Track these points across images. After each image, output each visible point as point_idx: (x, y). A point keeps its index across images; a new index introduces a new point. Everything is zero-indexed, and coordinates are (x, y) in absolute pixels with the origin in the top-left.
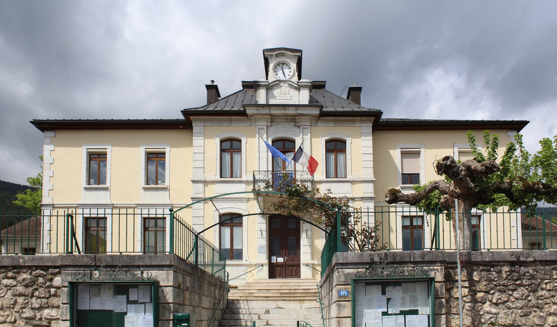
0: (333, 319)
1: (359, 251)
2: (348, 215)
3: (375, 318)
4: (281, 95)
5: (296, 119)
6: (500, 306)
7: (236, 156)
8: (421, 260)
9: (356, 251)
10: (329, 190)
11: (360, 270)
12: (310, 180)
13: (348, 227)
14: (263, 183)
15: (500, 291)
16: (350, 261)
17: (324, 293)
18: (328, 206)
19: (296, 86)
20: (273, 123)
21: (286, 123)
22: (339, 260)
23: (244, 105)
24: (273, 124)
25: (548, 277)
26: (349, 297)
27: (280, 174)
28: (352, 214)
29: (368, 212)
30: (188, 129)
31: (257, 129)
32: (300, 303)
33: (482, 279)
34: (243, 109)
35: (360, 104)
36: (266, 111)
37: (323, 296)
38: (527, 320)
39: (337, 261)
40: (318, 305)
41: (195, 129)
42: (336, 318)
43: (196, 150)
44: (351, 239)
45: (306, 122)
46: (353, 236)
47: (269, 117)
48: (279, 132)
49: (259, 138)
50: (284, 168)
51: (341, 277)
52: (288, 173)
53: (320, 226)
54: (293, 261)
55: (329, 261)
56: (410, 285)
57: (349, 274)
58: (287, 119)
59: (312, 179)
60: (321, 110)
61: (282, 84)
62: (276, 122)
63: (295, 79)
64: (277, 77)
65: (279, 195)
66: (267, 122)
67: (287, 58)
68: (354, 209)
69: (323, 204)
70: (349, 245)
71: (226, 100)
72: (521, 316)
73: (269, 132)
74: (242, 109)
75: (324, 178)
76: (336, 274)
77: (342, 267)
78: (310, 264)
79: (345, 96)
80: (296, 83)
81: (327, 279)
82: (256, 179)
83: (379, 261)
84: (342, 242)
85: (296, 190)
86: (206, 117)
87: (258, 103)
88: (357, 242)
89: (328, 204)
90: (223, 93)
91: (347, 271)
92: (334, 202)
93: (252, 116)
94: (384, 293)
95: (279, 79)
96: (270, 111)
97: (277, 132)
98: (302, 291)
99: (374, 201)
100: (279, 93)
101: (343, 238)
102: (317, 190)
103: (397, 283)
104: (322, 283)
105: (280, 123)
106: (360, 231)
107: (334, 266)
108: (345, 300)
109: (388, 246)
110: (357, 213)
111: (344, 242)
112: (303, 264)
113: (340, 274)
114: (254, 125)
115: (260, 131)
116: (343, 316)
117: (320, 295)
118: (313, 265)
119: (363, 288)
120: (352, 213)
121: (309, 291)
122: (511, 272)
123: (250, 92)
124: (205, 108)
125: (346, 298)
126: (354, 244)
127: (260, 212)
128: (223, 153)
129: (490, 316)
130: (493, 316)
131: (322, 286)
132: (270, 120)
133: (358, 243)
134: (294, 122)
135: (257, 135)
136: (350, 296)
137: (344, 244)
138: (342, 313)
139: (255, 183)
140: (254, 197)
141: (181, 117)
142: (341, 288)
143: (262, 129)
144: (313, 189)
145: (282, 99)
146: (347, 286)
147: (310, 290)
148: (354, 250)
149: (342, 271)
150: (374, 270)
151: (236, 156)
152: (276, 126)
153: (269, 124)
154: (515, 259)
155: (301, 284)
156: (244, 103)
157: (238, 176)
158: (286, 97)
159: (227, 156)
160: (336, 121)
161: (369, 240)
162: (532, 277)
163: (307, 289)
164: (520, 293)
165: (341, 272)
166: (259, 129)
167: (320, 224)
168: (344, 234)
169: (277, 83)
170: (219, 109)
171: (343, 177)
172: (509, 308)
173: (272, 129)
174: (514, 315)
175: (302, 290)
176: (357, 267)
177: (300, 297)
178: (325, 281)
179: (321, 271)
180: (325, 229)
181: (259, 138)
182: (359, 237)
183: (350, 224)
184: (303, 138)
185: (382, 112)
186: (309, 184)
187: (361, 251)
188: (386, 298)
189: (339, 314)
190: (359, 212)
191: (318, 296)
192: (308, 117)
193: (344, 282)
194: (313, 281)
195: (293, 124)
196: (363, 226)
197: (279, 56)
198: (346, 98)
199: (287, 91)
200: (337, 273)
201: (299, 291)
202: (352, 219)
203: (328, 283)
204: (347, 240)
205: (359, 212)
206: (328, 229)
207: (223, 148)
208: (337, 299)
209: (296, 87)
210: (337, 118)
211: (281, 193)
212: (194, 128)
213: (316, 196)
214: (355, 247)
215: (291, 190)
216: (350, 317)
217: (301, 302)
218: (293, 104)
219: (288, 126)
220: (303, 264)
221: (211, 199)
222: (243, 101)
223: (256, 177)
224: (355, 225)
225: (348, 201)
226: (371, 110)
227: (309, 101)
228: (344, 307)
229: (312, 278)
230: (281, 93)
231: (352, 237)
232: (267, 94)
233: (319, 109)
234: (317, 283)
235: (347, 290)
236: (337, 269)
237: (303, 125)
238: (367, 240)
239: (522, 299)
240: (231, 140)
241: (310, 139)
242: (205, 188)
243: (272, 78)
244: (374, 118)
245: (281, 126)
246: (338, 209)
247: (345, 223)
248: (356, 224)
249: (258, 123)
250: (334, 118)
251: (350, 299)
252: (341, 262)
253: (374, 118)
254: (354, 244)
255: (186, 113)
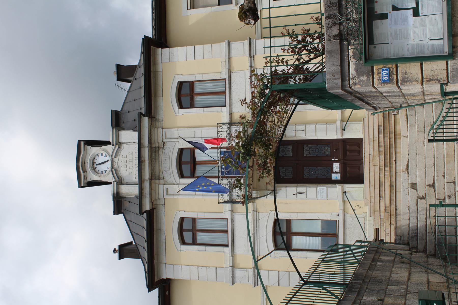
0: (425, 89)
1: (324, 56)
2: (274, 74)
3: (424, 26)
4: (128, 166)
5: (155, 148)
7: (200, 224)
9: (324, 60)
10: (242, 103)
11: (351, 54)
12: (229, 128)
13: (291, 73)
14: (234, 191)
16: (338, 69)
17: (384, 104)
18: (263, 102)
19: (117, 147)
20: (160, 176)
22: (337, 84)
23: (140, 213)
26: (392, 67)
27: (222, 168)
28: (273, 69)
29: (271, 47)
30: (169, 284)
31: (167, 197)
32: (400, 138)
34: (145, 214)
35: (136, 66)
36: (147, 185)
37: (389, 105)
39: (339, 88)
40: (402, 112)
41: (170, 276)
42: (422, 85)
43: (194, 277)
44: (307, 69)
45: (159, 134)
46: (302, 67)
47: (153, 180)
48: (171, 169)
49: (179, 195)
50: (214, 162)
51: (361, 81)
52: (221, 157)
53: (289, 112)
54: (339, 149)
55: (337, 98)
57: (356, 70)
58: (155, 159)
59: (227, 125)
60: (144, 116)
61: (116, 166)
62: (159, 173)
63: (109, 148)
64: (108, 170)
65: (249, 170)
66: (159, 184)
67: (87, 159)
68: (267, 66)
69: (260, 110)
70: (316, 70)
71: (135, 235)
73: (171, 182)
74: (145, 215)
75: (225, 110)
76: (357, 88)
77: (347, 79)
78: (341, 125)
79: (127, 85)
80: (114, 147)
81: (363, 101)
82: (229, 199)
83: (338, 26)
84: (311, 80)
85: (243, 146)
86: (155, 261)
87: (138, 195)
88: (311, 59)
89: (260, 103)
90: (127, 238)
91: (352, 71)
92: (258, 95)
93: (153, 203)
95: (110, 169)
96: (147, 181)
97: (171, 171)
98: (382, 136)
99: (254, 40)
100: (126, 169)
101: (305, 79)
102: (243, 118)
104: (370, 108)
105: (160, 168)
106: (296, 57)
107: (346, 91)
108: (395, 73)
109: (316, 16)
110: (271, 62)
111: (312, 78)
112: (342, 135)
113: (357, 82)
114: (163, 200)
115: (170, 193)
116: (420, 75)
117: (387, 109)
118: (342, 121)
119: (377, 48)
120: (271, 68)
121: (381, 126)
123: (126, 205)
124: (145, 262)
125: (392, 72)
126: (314, 65)
127: (271, 195)
128: (198, 242)
131: (374, 107)
132: (157, 181)
133: (313, 59)
134: (159, 150)
135: (175, 197)
136: (390, 66)
137: (314, 78)
138: (415, 77)
139: (234, 200)
140: (252, 203)
141: (156, 292)
142: (378, 80)
143: (167, 191)
144: (241, 124)
145: (132, 165)
146: (375, 71)
147: (380, 124)
148: (323, 63)
149: (353, 79)
150: (350, 33)
151: (200, 224)
152: (164, 172)
153: (162, 181)
155: (371, 137)
156: (138, 213)
157: (225, 223)
158: (130, 161)
159: (201, 237)
160: (156, 96)
161: (307, 43)
163: (379, 129)
165: (354, 81)
166: (167, 194)
167: (287, 113)
168: (300, 79)
169: (114, 170)
170: (145, 245)
171: (224, 83)
173: (167, 178)
175: (380, 136)
176: (346, 58)
177: (390, 138)
178: (367, 103)
179: (351, 110)
180: (294, 106)
181: (179, 195)
182: (304, 57)
183: (286, 71)
184: (178, 138)
185: (145, 36)
186: (233, 129)
187: (324, 54)
188: (392, 12)
189: (417, 81)
190: (271, 59)
191: (389, 113)
192: (152, 132)
193: (368, 75)
194: (366, 120)
195: (161, 150)
196: (288, 52)
197: (85, 169)
198: (130, 84)
199: (123, 159)
200: (356, 87)
201: (382, 140)
202: (280, 69)
203: (370, 99)
204: (309, 74)
205: (271, 59)
206: (294, 101)
207: (191, 242)
208: (395, 85)
209: (119, 148)
210: (153, 95)
211: (247, 167)
212: (169, 277)
213: (250, 119)
214: (319, 63)
215: (243, 154)
216: (421, 64)
217: (398, 137)
218: (138, 152)
219: (163, 157)
220: (342, 135)
221: (256, 262)
222: (136, 214)
223: (226, 200)
224: (287, 65)
225: (256, 75)
226: (143, 51)
227: (135, 131)
228: (406, 73)
229: (362, 122)
230: (125, 166)
231: (305, 67)
232: (127, 184)
233: (143, 117)
234: (370, 115)
235: (380, 71)
236: (349, 87)
237: (162, 138)
238: (308, 46)
240: (181, 231)
241: (179, 129)
242: (241, 266)
243: (109, 178)
244: (152, 47)
245: (164, 166)
246: (266, 89)
247: (285, 77)
248: (287, 63)
249: (161, 197)
250: (152, 98)
251: (394, 66)
252: (339, 81)
253: (152, 47)
254: (314, 65)
255: (151, 287)
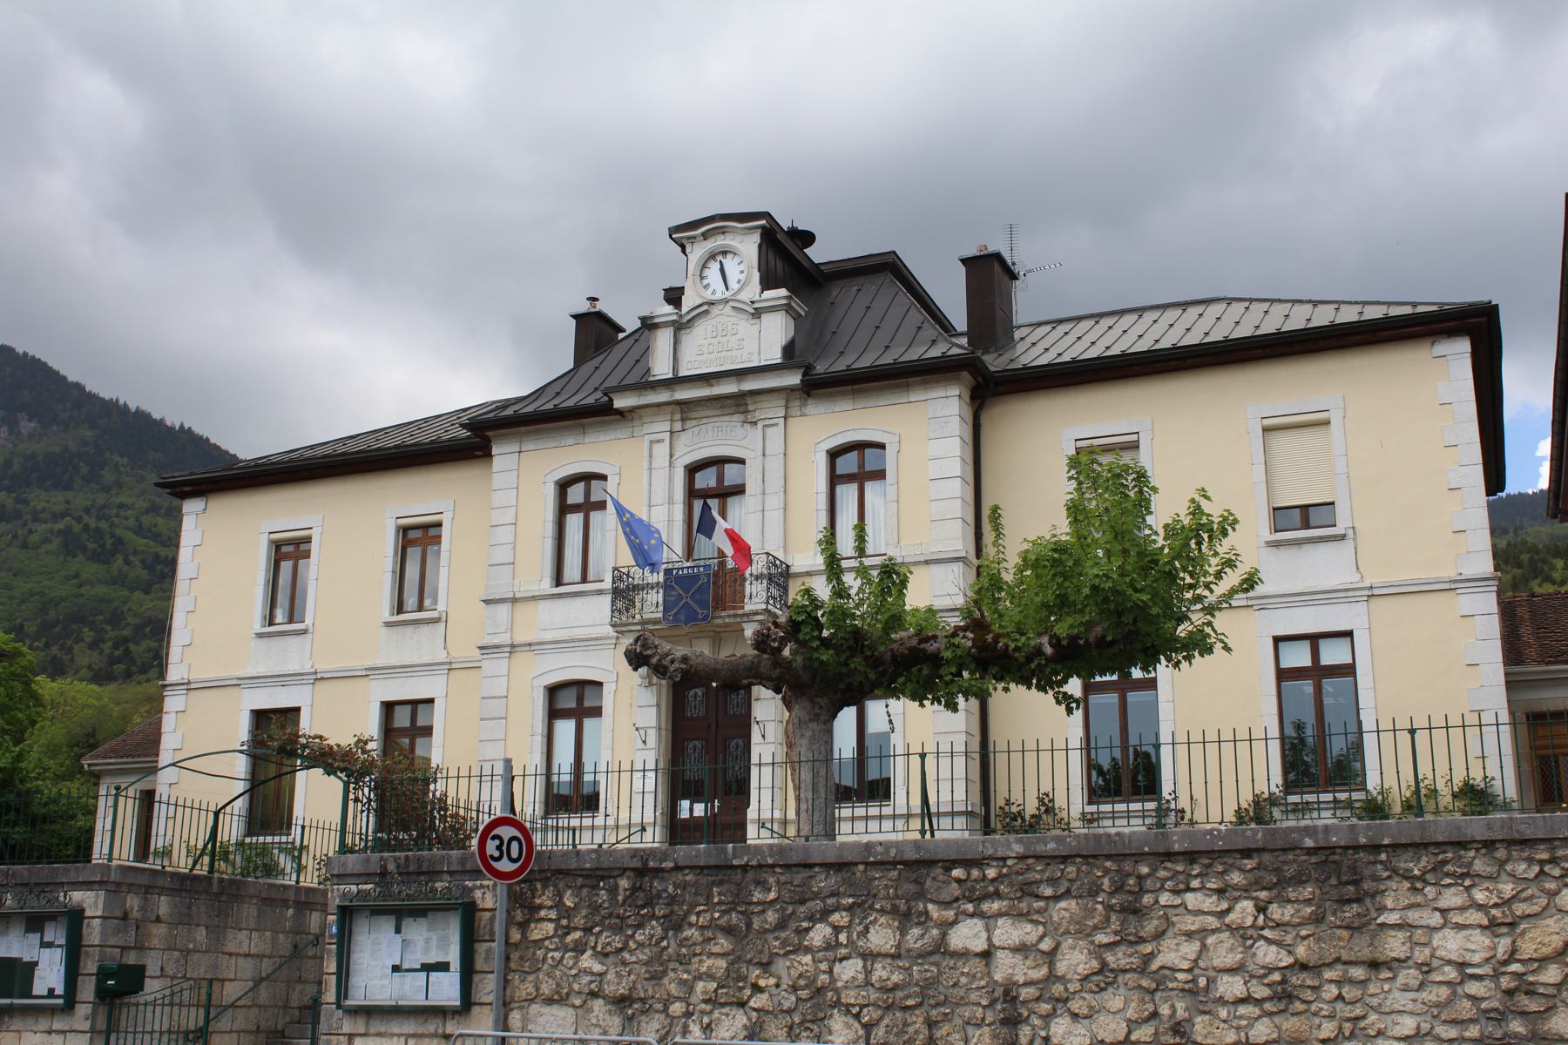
6: (611, 959)
8: (459, 868)
15: (610, 927)
21: (722, 418)
24: (689, 424)
25: (702, 900)
33: (583, 903)
38: (657, 988)
48: (701, 445)
56: (440, 914)
72: (646, 979)
94: (398, 931)
103: (419, 912)
105: (705, 421)
122: (634, 889)
129: (589, 978)
130: (593, 978)
152: (696, 430)
154: (639, 865)
162: (672, 900)
164: (647, 933)
172: (624, 963)
174: (632, 977)
239: (650, 945)
